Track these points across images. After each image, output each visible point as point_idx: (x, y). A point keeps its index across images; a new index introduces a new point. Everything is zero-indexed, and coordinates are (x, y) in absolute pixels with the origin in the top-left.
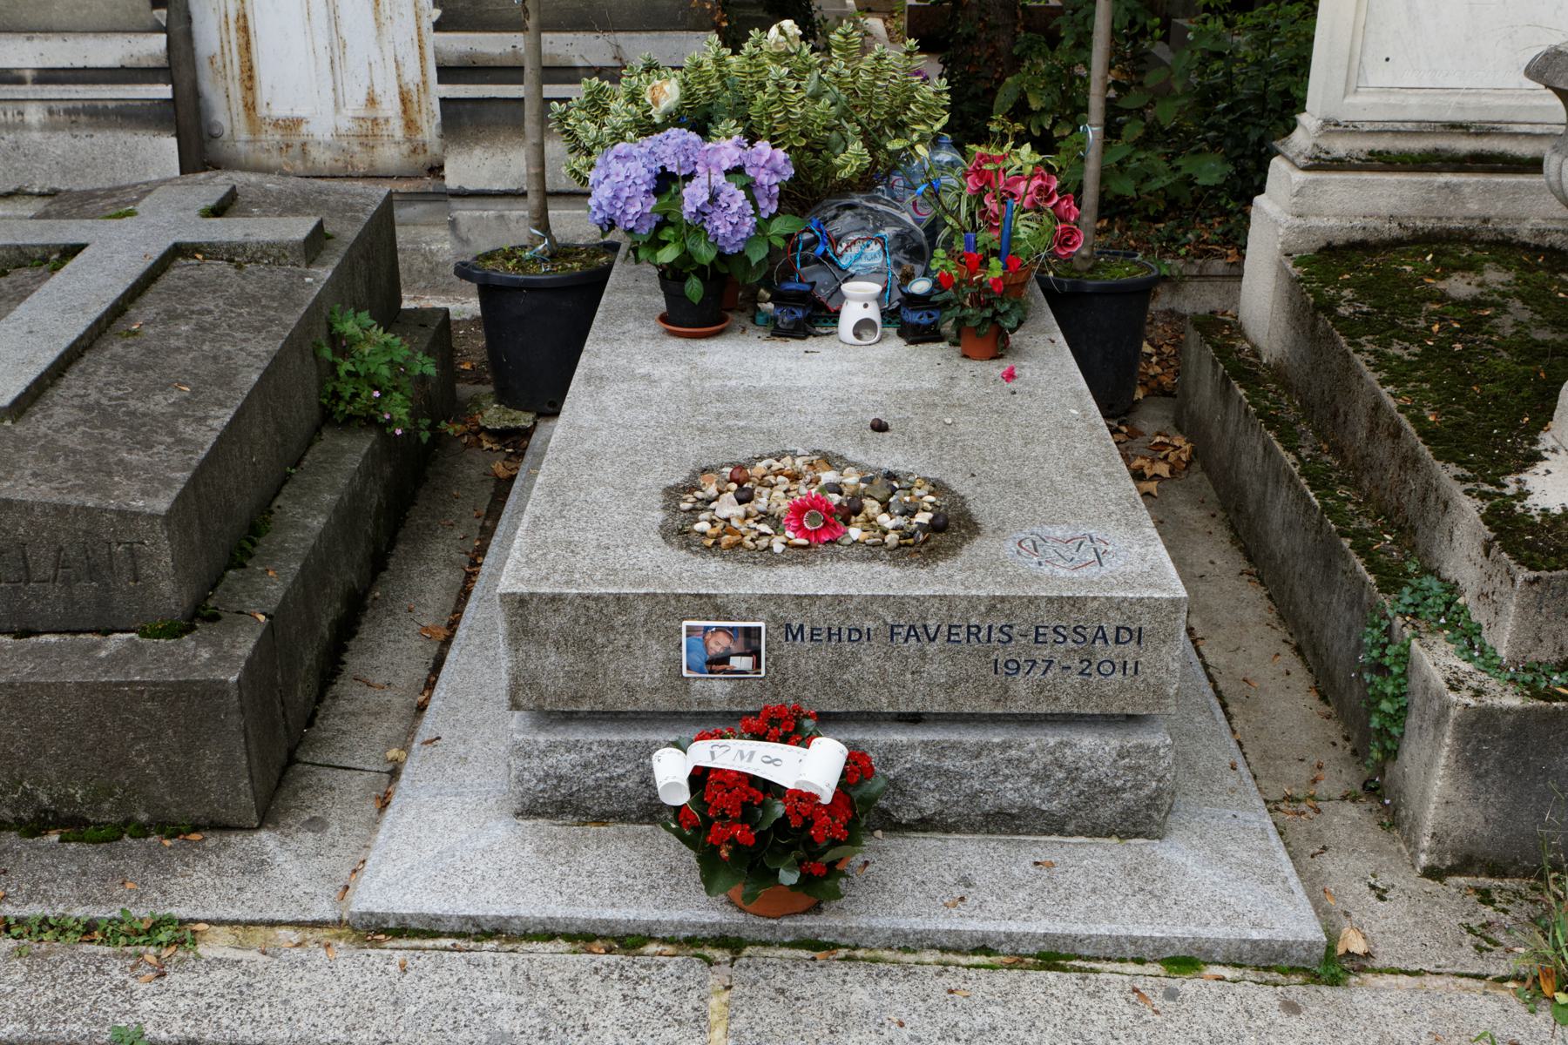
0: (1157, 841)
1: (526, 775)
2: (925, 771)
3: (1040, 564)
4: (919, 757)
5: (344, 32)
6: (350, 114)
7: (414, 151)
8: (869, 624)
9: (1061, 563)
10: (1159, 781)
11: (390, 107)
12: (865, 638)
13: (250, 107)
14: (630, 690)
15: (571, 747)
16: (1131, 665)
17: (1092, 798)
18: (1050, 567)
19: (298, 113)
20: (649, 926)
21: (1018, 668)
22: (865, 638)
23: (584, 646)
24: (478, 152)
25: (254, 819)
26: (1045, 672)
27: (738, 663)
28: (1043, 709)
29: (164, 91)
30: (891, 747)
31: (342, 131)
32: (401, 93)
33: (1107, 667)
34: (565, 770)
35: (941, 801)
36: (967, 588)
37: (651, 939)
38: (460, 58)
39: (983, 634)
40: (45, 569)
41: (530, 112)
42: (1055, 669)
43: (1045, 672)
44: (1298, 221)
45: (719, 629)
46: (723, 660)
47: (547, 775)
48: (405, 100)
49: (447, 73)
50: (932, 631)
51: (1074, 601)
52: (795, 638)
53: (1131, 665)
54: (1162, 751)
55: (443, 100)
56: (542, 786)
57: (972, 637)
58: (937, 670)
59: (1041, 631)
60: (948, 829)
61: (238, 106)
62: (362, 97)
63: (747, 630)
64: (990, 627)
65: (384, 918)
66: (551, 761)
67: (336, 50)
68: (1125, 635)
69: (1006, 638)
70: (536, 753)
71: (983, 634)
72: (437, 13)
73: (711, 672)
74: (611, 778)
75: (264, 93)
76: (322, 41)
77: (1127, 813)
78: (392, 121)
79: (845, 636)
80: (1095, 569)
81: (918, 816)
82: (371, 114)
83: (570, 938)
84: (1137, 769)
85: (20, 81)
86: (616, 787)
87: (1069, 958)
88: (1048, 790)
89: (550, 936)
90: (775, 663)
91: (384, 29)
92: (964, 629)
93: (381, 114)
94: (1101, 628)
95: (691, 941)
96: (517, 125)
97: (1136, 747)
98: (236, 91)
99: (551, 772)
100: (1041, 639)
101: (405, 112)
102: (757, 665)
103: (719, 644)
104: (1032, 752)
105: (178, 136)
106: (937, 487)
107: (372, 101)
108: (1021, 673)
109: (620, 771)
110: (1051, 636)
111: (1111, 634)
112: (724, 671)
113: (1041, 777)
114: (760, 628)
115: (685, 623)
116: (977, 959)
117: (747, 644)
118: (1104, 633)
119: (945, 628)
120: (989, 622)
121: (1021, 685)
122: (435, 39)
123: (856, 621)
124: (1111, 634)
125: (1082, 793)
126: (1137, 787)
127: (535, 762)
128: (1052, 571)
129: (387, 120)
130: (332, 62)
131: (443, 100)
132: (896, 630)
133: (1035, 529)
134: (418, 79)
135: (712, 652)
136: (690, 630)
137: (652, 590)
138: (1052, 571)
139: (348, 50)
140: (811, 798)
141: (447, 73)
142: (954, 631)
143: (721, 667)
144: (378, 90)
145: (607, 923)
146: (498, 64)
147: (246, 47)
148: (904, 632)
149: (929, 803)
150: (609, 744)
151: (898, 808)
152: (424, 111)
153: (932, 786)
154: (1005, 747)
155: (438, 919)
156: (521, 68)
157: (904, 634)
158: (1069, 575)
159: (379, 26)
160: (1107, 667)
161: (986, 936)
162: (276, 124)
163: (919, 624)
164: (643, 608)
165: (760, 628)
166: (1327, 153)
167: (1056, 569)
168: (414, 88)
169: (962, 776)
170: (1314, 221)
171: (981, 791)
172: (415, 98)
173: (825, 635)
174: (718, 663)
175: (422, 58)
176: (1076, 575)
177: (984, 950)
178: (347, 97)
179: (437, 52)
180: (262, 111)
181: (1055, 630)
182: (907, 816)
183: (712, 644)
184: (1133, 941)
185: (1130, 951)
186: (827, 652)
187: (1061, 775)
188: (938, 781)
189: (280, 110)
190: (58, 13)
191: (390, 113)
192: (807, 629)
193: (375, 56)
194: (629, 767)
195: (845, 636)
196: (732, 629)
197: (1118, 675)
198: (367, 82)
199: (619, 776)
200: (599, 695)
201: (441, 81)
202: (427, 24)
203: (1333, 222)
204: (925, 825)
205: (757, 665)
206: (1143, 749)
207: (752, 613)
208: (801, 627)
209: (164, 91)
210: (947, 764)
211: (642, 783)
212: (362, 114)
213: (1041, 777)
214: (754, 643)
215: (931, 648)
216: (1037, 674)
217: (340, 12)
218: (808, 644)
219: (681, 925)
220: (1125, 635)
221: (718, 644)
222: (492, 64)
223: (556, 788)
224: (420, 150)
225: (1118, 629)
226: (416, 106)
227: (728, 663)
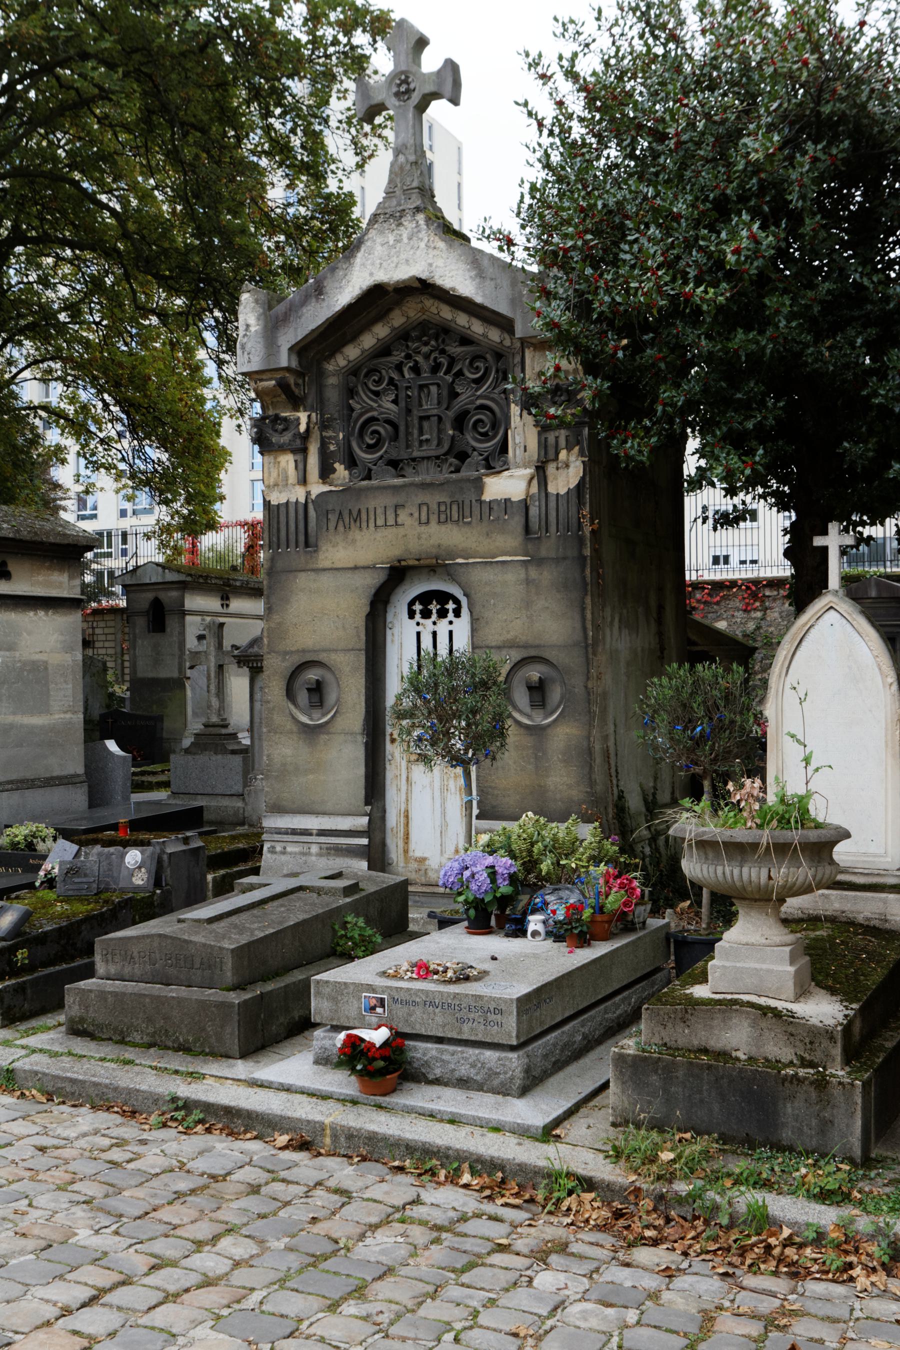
2: (437, 1059)
4: (434, 1053)
5: (448, 819)
8: (418, 1000)
13: (406, 851)
14: (348, 1018)
17: (490, 1076)
19: (425, 855)
20: (332, 1093)
23: (334, 1000)
25: (238, 1056)
28: (473, 1038)
29: (365, 841)
30: (426, 1049)
34: (327, 1046)
40: (197, 965)
51: (480, 996)
58: (439, 1019)
60: (446, 1084)
61: (401, 851)
62: (453, 849)
65: (257, 1080)
75: (412, 846)
76: (438, 823)
77: (503, 1084)
83: (309, 1094)
84: (504, 1065)
85: (311, 834)
89: (303, 1093)
90: (390, 1012)
95: (344, 1100)
98: (401, 844)
103: (373, 1002)
105: (369, 862)
113: (473, 1066)
121: (466, 1028)
123: (414, 998)
126: (505, 1073)
140: (373, 1045)
145: (319, 1090)
147: (407, 824)
149: (438, 1072)
154: (462, 1052)
155: (272, 1082)
161: (432, 1111)
162: (416, 860)
164: (352, 987)
169: (449, 1062)
174: (373, 1009)
177: (431, 1116)
180: (411, 854)
182: (431, 1077)
184: (479, 1118)
186: (405, 1009)
189: (418, 854)
190: (329, 807)
200: (339, 1019)
204: (437, 1082)
206: (507, 1058)
207: (383, 992)
209: (365, 841)
210: (444, 1057)
213: (473, 1066)
215: (437, 1010)
216: (470, 1024)
219: (341, 1094)
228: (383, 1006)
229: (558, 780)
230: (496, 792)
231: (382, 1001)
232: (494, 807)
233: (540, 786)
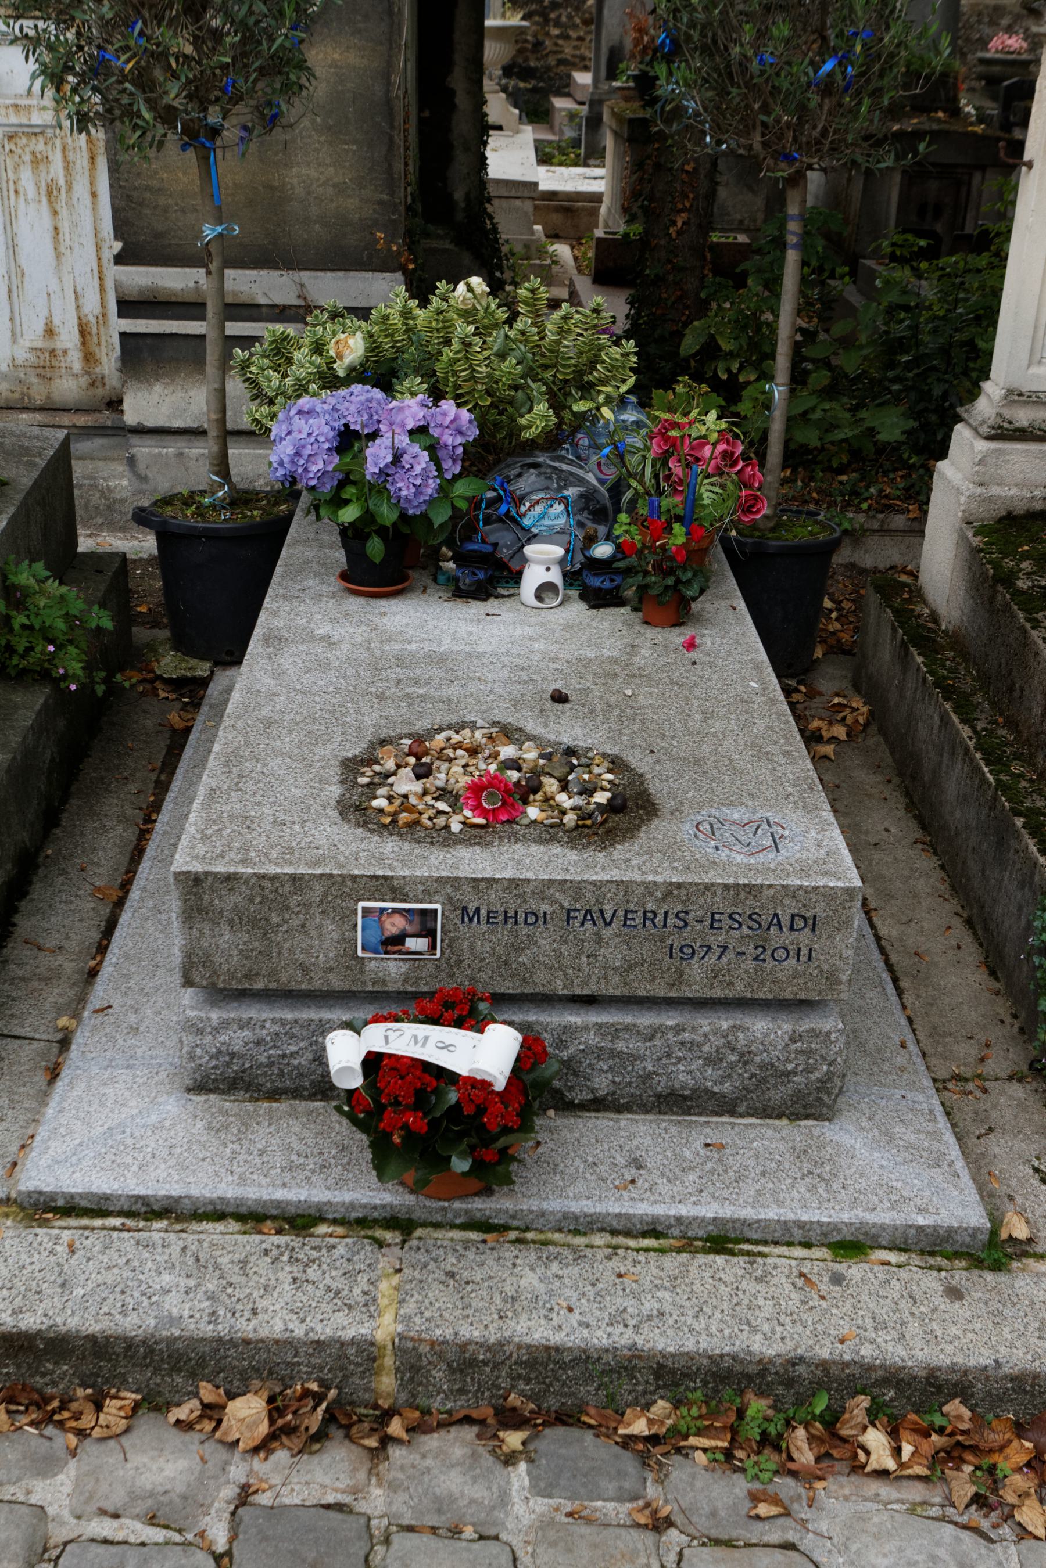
0: (827, 1123)
1: (198, 1051)
2: (599, 1053)
3: (717, 848)
4: (592, 1038)
5: (23, 261)
6: (28, 344)
7: (93, 384)
8: (545, 907)
9: (738, 847)
10: (830, 1065)
11: (68, 338)
12: (541, 921)
14: (305, 969)
15: (243, 1025)
16: (804, 951)
17: (764, 1080)
18: (727, 852)
20: (319, 1206)
21: (693, 954)
22: (541, 921)
23: (259, 925)
24: (158, 388)
26: (720, 958)
27: (415, 944)
28: (717, 993)
30: (566, 1029)
31: (19, 361)
32: (80, 325)
33: (781, 954)
34: (237, 1047)
35: (614, 1082)
36: (644, 873)
37: (321, 1219)
38: (141, 292)
39: (660, 918)
41: (212, 353)
42: (730, 955)
43: (720, 958)
44: (979, 490)
45: (395, 911)
46: (398, 940)
47: (220, 1052)
48: (84, 332)
49: (128, 307)
50: (608, 916)
51: (750, 888)
52: (471, 920)
53: (804, 951)
54: (833, 1036)
55: (123, 335)
56: (214, 1063)
57: (648, 922)
58: (613, 954)
59: (717, 917)
60: (620, 1109)
62: (40, 327)
63: (423, 912)
64: (666, 913)
65: (53, 1196)
66: (224, 1038)
67: (13, 278)
68: (799, 923)
69: (682, 923)
70: (209, 1030)
71: (660, 918)
72: (118, 246)
73: (386, 953)
74: (284, 1056)
77: (797, 1096)
78: (70, 353)
79: (521, 919)
80: (772, 855)
81: (590, 1096)
82: (48, 345)
83: (240, 1218)
84: (808, 1053)
86: (288, 1064)
87: (738, 1241)
88: (720, 1072)
90: (451, 944)
91: (63, 259)
92: (640, 914)
93: (59, 346)
94: (776, 915)
95: (362, 1223)
96: (198, 362)
97: (808, 1031)
99: (224, 1048)
100: (716, 925)
101: (83, 344)
102: (433, 946)
103: (395, 925)
104: (705, 1035)
106: (616, 764)
107: (50, 332)
108: (696, 958)
109: (293, 1049)
110: (726, 922)
111: (785, 921)
112: (400, 952)
113: (713, 1060)
114: (436, 911)
115: (361, 904)
116: (647, 1242)
117: (423, 923)
118: (779, 921)
119: (621, 913)
120: (665, 907)
121: (696, 970)
122: (115, 272)
123: (532, 904)
124: (785, 921)
125: (753, 1075)
126: (809, 1070)
127: (208, 1039)
128: (729, 856)
129: (65, 352)
130: (10, 291)
131: (123, 335)
132: (572, 914)
133: (713, 811)
134: (98, 310)
135: (388, 934)
136: (366, 910)
137: (328, 871)
138: (729, 856)
139: (26, 279)
140: (485, 1085)
141: (128, 307)
142: (630, 916)
143: (396, 948)
144: (56, 321)
146: (180, 300)
148: (580, 916)
149: (602, 1084)
150: (282, 1022)
151: (571, 1089)
152: (103, 343)
153: (605, 1068)
154: (678, 1029)
155: (107, 1198)
156: (204, 305)
157: (580, 918)
158: (745, 861)
159: (58, 255)
160: (781, 954)
161: (656, 1220)
163: (595, 908)
164: (318, 888)
165: (436, 911)
166: (1010, 423)
167: (733, 855)
168: (93, 320)
169: (637, 1058)
170: (995, 490)
171: (654, 1073)
172: (94, 330)
173: (501, 918)
175: (102, 289)
176: (752, 861)
178: (25, 327)
179: (118, 287)
181: (730, 917)
182: (579, 1096)
183: (388, 925)
184: (801, 1225)
185: (798, 1235)
186: (503, 935)
187: (733, 1058)
188: (611, 1062)
191: (68, 345)
192: (483, 912)
193: (54, 285)
194: (302, 1044)
195: (521, 919)
196: (408, 911)
197: (792, 962)
198: (46, 313)
199: (292, 1054)
200: (273, 973)
201: (121, 315)
202: (108, 255)
203: (1013, 491)
204: (598, 1105)
205: (433, 946)
206: (814, 1034)
207: (428, 895)
208: (478, 910)
210: (621, 1046)
211: (314, 1060)
212: (39, 344)
213: (713, 1060)
214: (430, 925)
215: (607, 933)
216: (712, 959)
217: (18, 240)
218: (484, 927)
219: (352, 1206)
220: (799, 923)
221: (393, 925)
222: (174, 299)
223: (228, 1064)
224: (98, 383)
225: (793, 916)
226: (95, 338)
227: (403, 944)
228: (430, 933)
229: (314, 174)
230: (162, 201)
231: (425, 920)
232: (159, 235)
233: (272, 188)
